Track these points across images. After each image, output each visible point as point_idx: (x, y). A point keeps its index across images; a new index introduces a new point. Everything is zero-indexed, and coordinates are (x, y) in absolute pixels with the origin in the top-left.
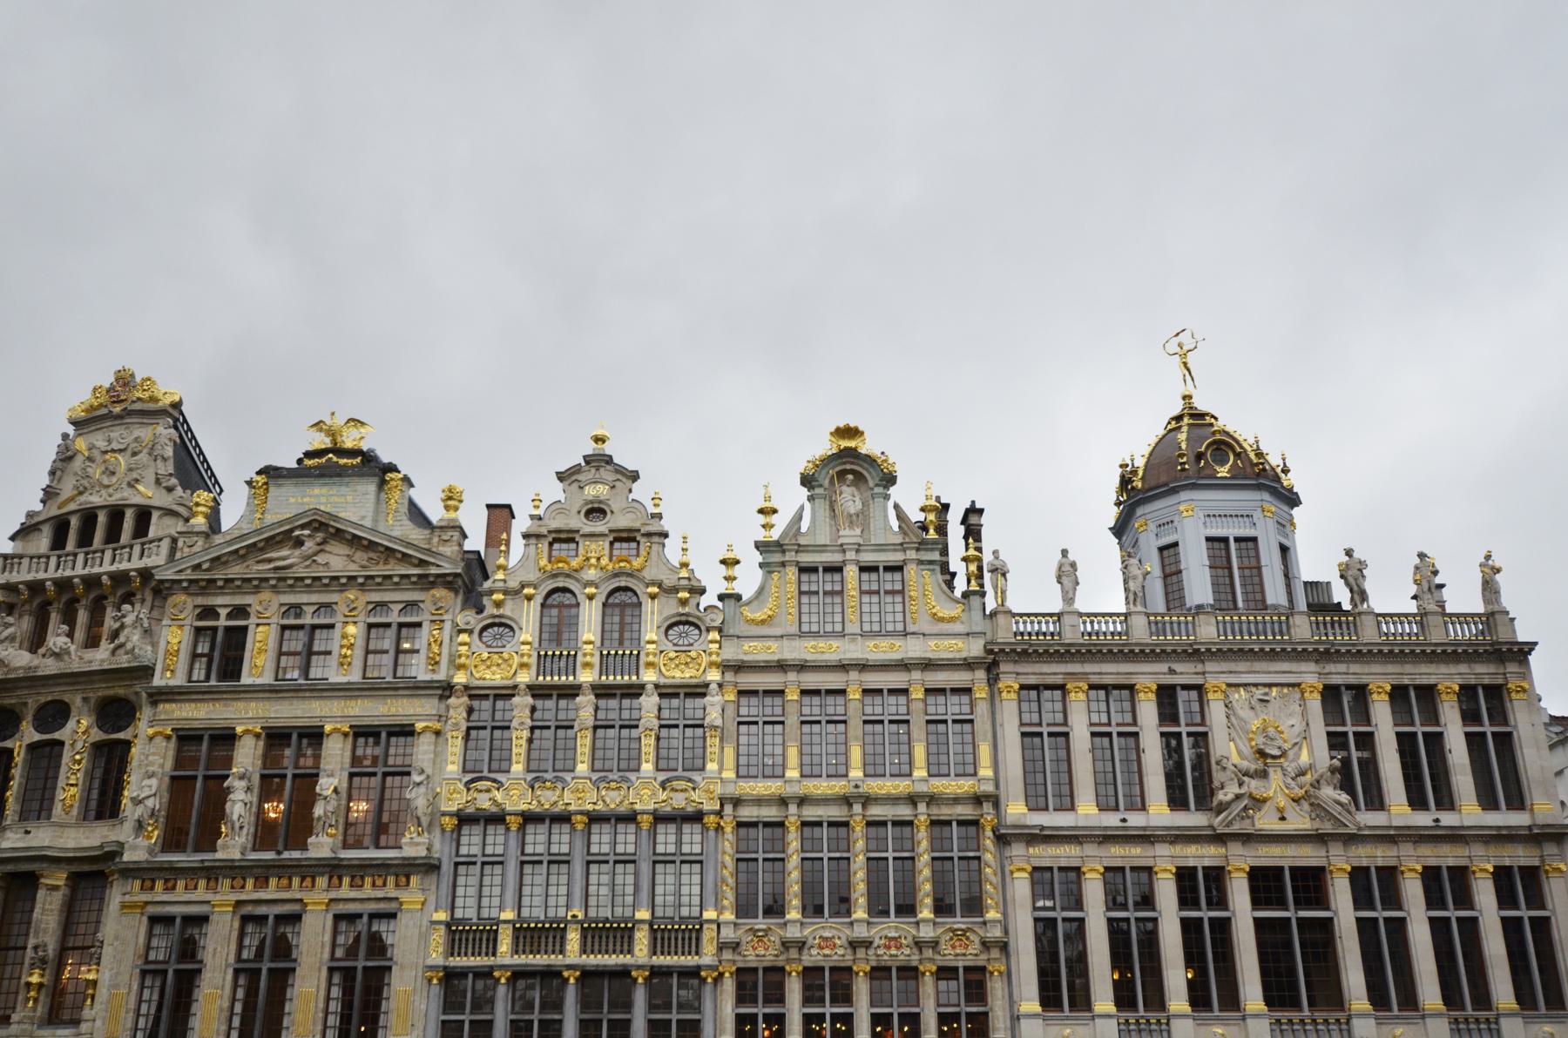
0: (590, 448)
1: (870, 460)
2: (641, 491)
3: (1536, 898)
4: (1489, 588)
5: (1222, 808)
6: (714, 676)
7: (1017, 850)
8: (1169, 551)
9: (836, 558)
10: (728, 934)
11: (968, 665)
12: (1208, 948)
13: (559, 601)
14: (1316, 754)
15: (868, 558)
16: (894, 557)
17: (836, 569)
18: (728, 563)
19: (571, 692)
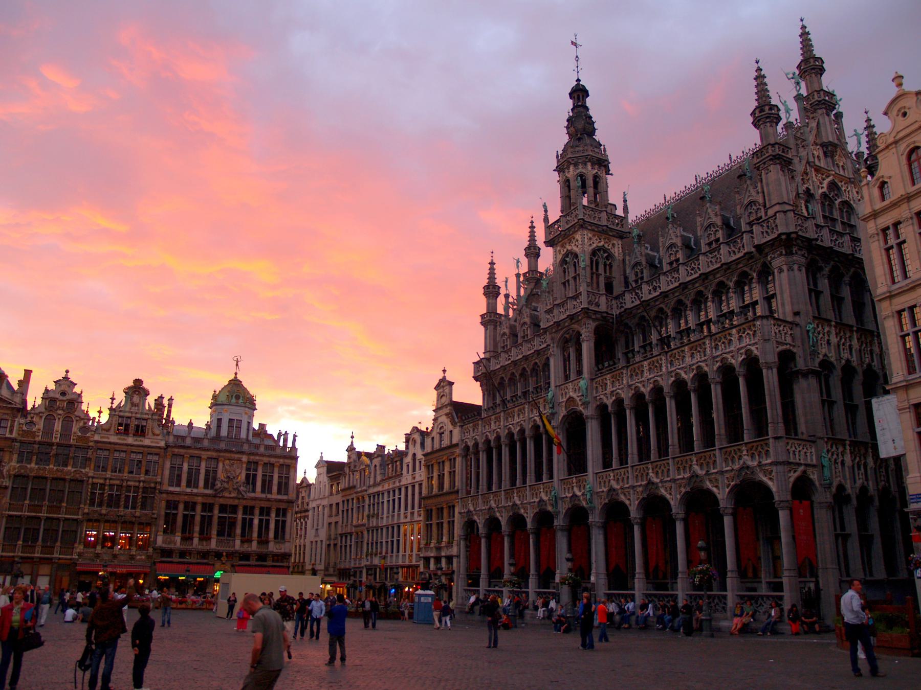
0: (64, 375)
1: (144, 389)
2: (77, 390)
3: (284, 515)
4: (294, 440)
5: (216, 490)
6: (91, 444)
7: (164, 495)
8: (219, 420)
9: (130, 415)
10: (86, 511)
11: (159, 448)
12: (206, 522)
13: (50, 419)
14: (243, 477)
15: (139, 416)
16: (147, 417)
17: (129, 418)
18: (100, 412)
19: (52, 444)
